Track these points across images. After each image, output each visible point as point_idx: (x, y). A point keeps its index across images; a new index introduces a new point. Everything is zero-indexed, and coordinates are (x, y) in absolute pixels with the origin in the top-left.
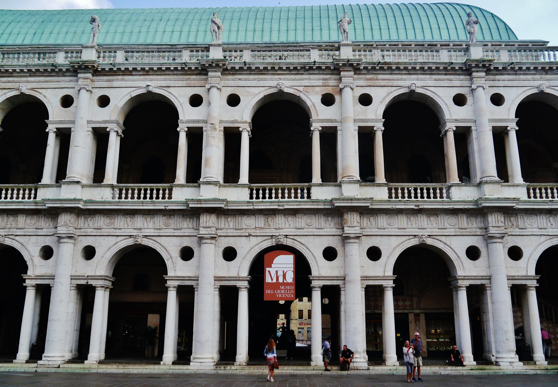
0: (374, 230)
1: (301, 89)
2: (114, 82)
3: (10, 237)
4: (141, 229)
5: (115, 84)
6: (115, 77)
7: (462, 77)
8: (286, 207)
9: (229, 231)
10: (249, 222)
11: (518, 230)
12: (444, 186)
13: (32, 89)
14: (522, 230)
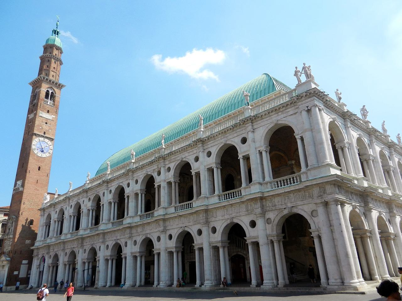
0: (170, 227)
5: (112, 185)
7: (196, 148)
8: (145, 223)
9: (135, 234)
11: (214, 218)
12: (191, 202)
14: (215, 219)
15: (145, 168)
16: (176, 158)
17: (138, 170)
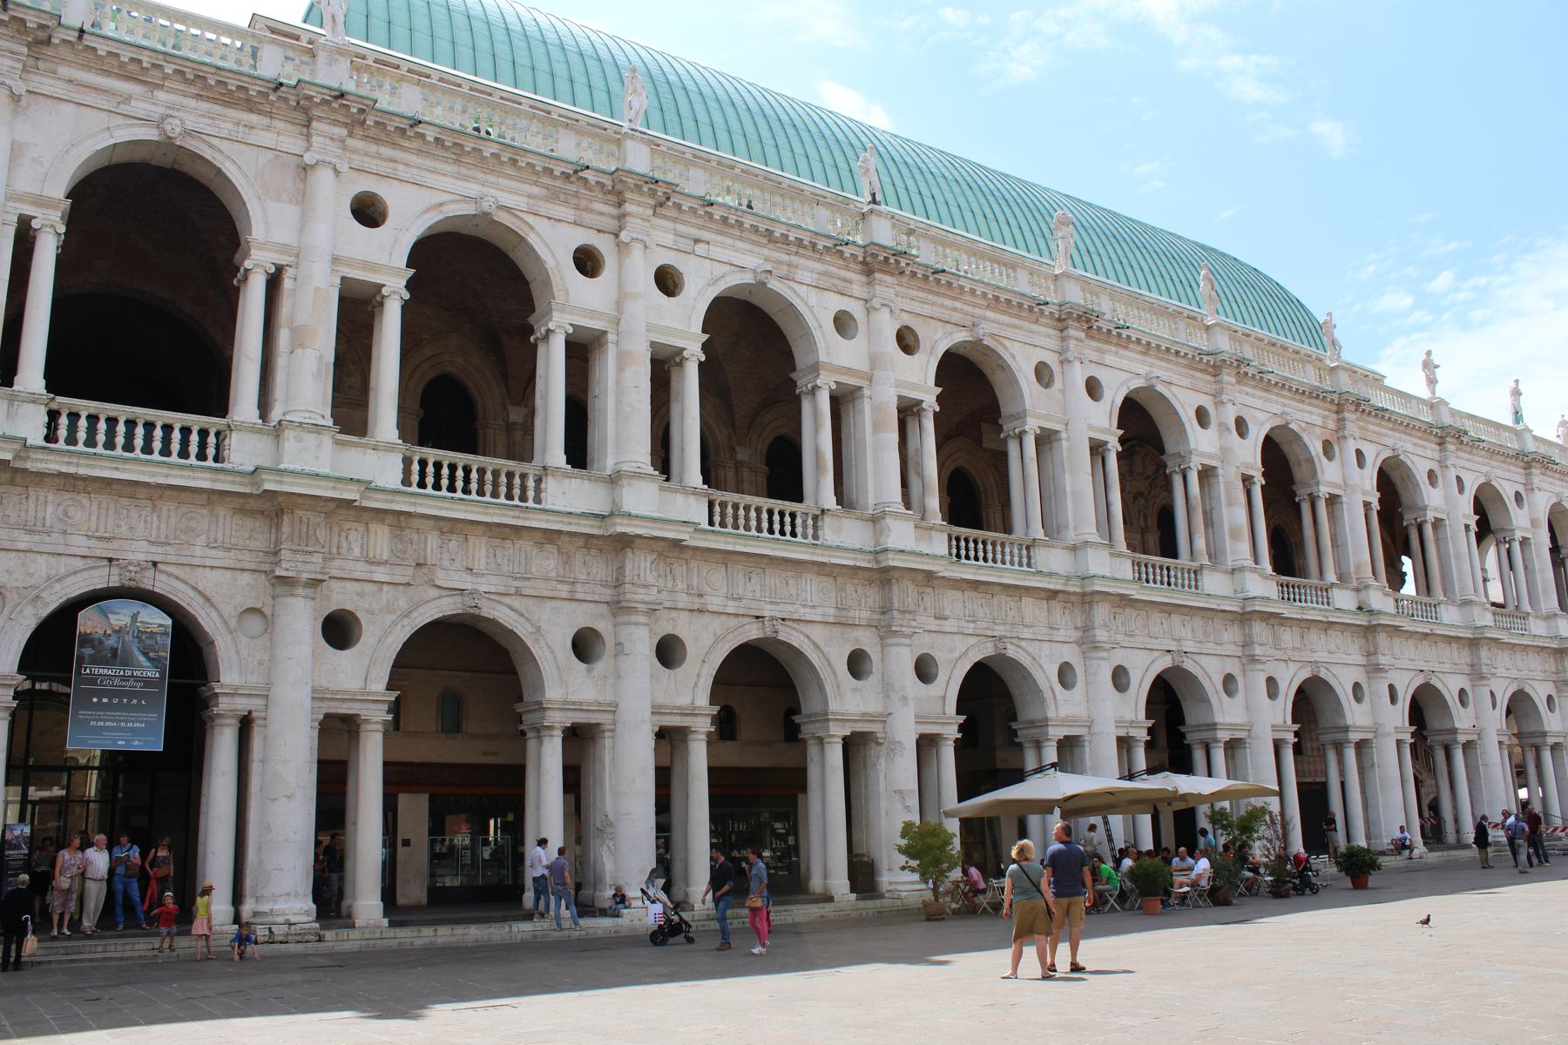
1: (1303, 425)
2: (1106, 356)
3: (1013, 640)
4: (1179, 640)
6: (1107, 347)
7: (1433, 446)
10: (1288, 637)
13: (992, 335)
15: (1277, 394)
16: (1386, 436)
17: (1252, 383)
